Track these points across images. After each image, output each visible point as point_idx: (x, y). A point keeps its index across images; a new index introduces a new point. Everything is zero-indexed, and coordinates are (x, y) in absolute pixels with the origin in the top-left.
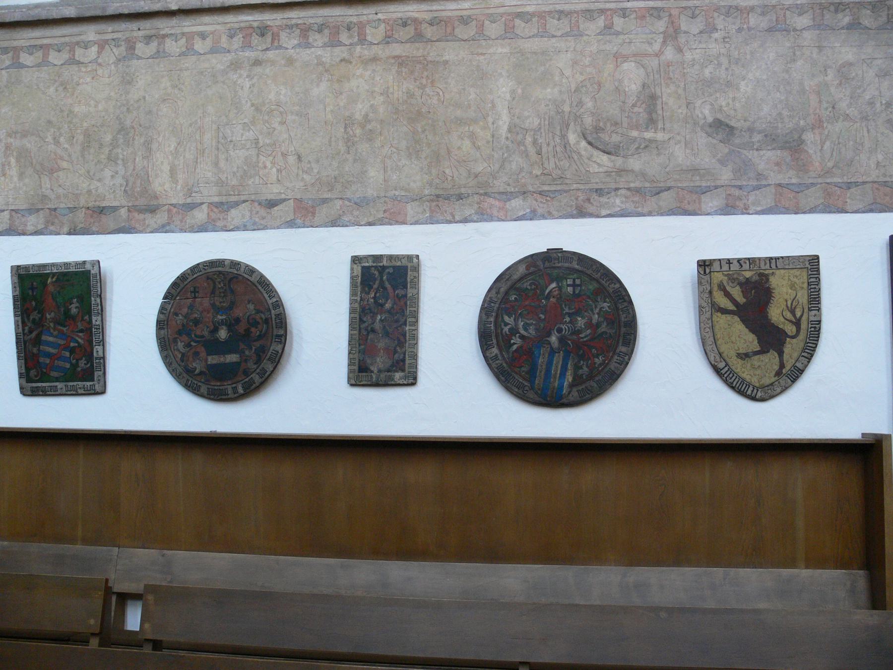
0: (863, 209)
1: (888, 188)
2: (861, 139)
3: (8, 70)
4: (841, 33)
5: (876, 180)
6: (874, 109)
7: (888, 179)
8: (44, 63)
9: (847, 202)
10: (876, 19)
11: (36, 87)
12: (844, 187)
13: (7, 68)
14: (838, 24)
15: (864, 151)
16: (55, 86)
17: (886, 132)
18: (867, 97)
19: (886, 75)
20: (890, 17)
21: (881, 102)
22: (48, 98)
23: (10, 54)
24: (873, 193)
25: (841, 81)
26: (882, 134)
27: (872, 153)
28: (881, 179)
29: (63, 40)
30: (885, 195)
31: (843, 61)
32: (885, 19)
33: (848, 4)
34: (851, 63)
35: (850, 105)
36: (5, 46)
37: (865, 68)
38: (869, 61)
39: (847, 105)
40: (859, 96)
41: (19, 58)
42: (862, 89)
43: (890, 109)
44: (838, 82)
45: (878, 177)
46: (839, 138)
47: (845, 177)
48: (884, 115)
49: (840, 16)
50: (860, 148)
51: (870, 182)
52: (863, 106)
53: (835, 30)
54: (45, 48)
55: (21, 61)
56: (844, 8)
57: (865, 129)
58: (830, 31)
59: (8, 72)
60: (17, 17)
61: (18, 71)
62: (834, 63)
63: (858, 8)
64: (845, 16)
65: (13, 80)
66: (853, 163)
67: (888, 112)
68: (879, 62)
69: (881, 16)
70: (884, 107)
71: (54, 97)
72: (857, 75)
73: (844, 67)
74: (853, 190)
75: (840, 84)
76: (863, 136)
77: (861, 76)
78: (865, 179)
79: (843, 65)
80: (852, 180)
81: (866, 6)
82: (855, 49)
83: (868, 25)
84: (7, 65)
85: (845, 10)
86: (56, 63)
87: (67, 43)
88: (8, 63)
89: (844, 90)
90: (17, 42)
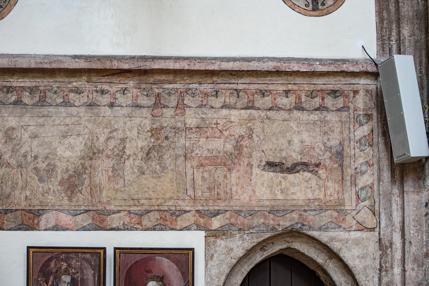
0: (15, 228)
1: (32, 215)
2: (16, 180)
4: (9, 107)
5: (24, 208)
6: (26, 160)
7: (32, 208)
9: (4, 223)
10: (32, 99)
12: (3, 213)
14: (8, 101)
15: (18, 189)
17: (32, 176)
18: (23, 152)
19: (35, 137)
20: (41, 98)
21: (31, 155)
24: (22, 217)
25: (6, 140)
26: (30, 177)
27: (22, 190)
28: (28, 208)
30: (30, 219)
31: (9, 126)
32: (37, 99)
33: (15, 88)
34: (14, 128)
35: (11, 157)
37: (22, 132)
38: (26, 127)
39: (9, 157)
40: (17, 151)
42: (20, 146)
43: (36, 161)
44: (4, 140)
45: (25, 206)
46: (2, 179)
47: (4, 206)
48: (32, 164)
49: (9, 95)
50: (15, 186)
51: (20, 210)
52: (20, 158)
53: (5, 104)
56: (12, 90)
57: (20, 174)
58: (2, 106)
62: (3, 128)
63: (21, 91)
64: (13, 95)
66: (10, 197)
67: (35, 163)
68: (32, 128)
69: (35, 97)
70: (33, 159)
72: (17, 136)
73: (10, 130)
74: (9, 215)
75: (6, 142)
76: (18, 178)
77: (20, 137)
78: (17, 207)
79: (9, 129)
80: (9, 208)
81: (26, 90)
82: (17, 119)
83: (27, 102)
85: (13, 91)
89: (8, 146)
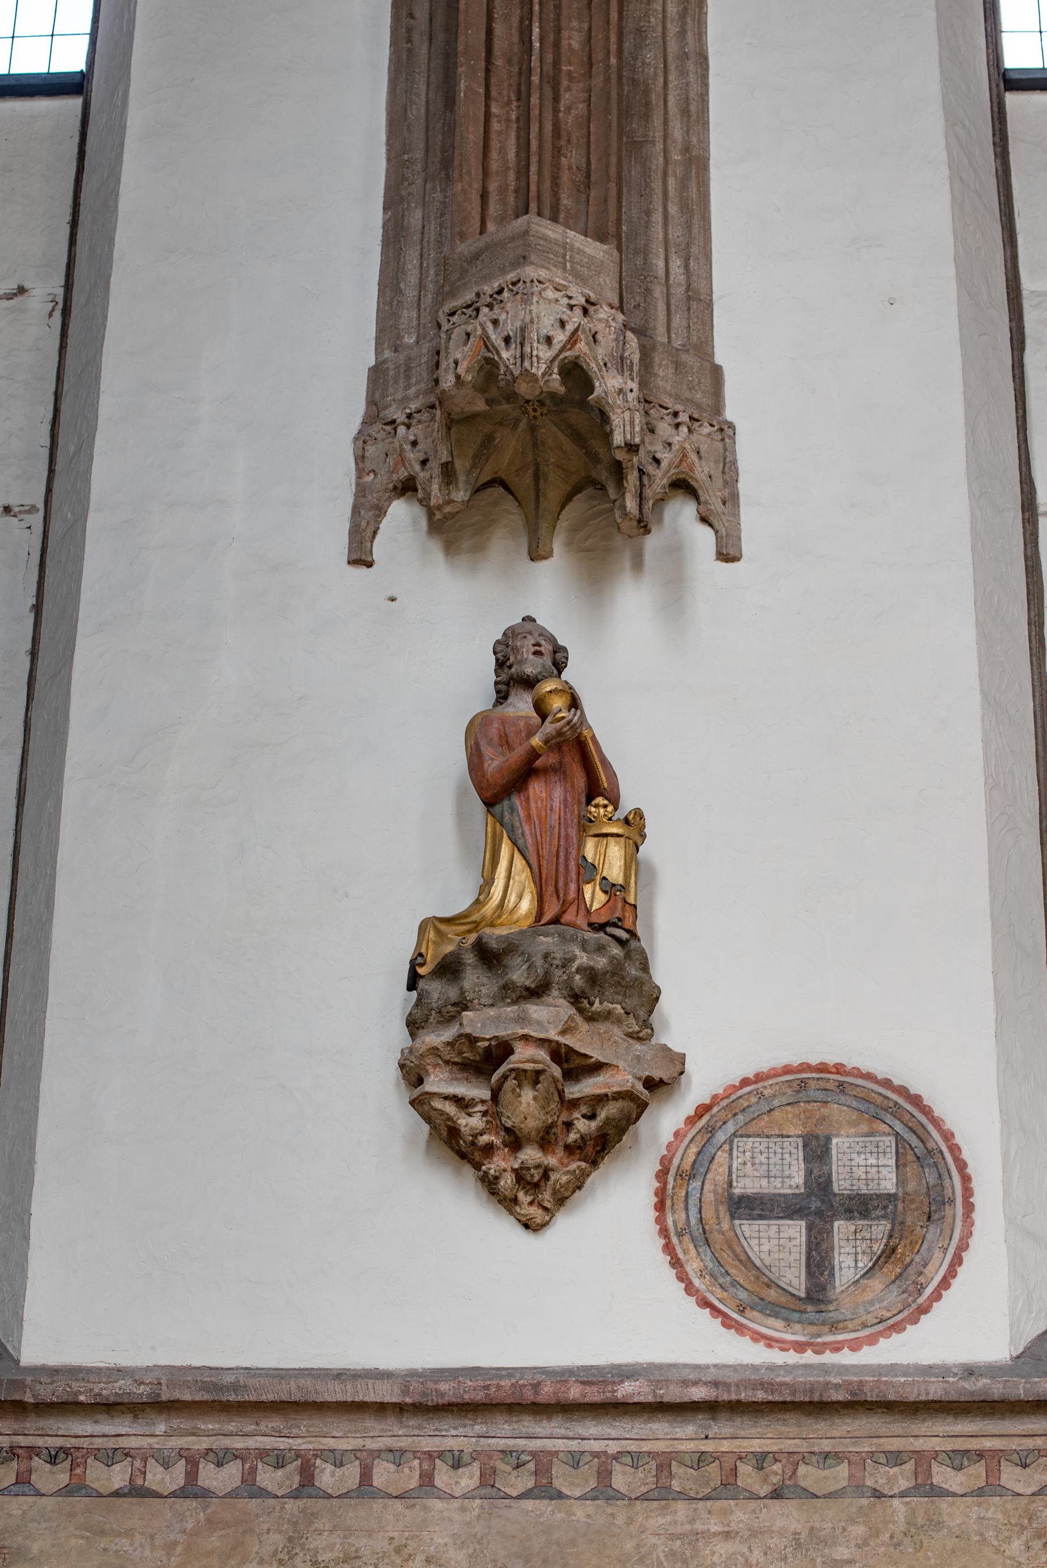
3: (908, 1499)
8: (990, 1489)
11: (976, 1538)
13: (903, 1495)
16: (1024, 1538)
22: (1008, 1562)
23: (909, 1466)
29: (1030, 1443)
36: (890, 1448)
41: (930, 1475)
54: (991, 1458)
55: (935, 1481)
59: (907, 1503)
60: (935, 1391)
61: (933, 1503)
65: (920, 1521)
71: (1022, 1560)
84: (902, 1489)
86: (1021, 1491)
87: (1039, 1450)
88: (903, 1484)
90: (921, 1440)
